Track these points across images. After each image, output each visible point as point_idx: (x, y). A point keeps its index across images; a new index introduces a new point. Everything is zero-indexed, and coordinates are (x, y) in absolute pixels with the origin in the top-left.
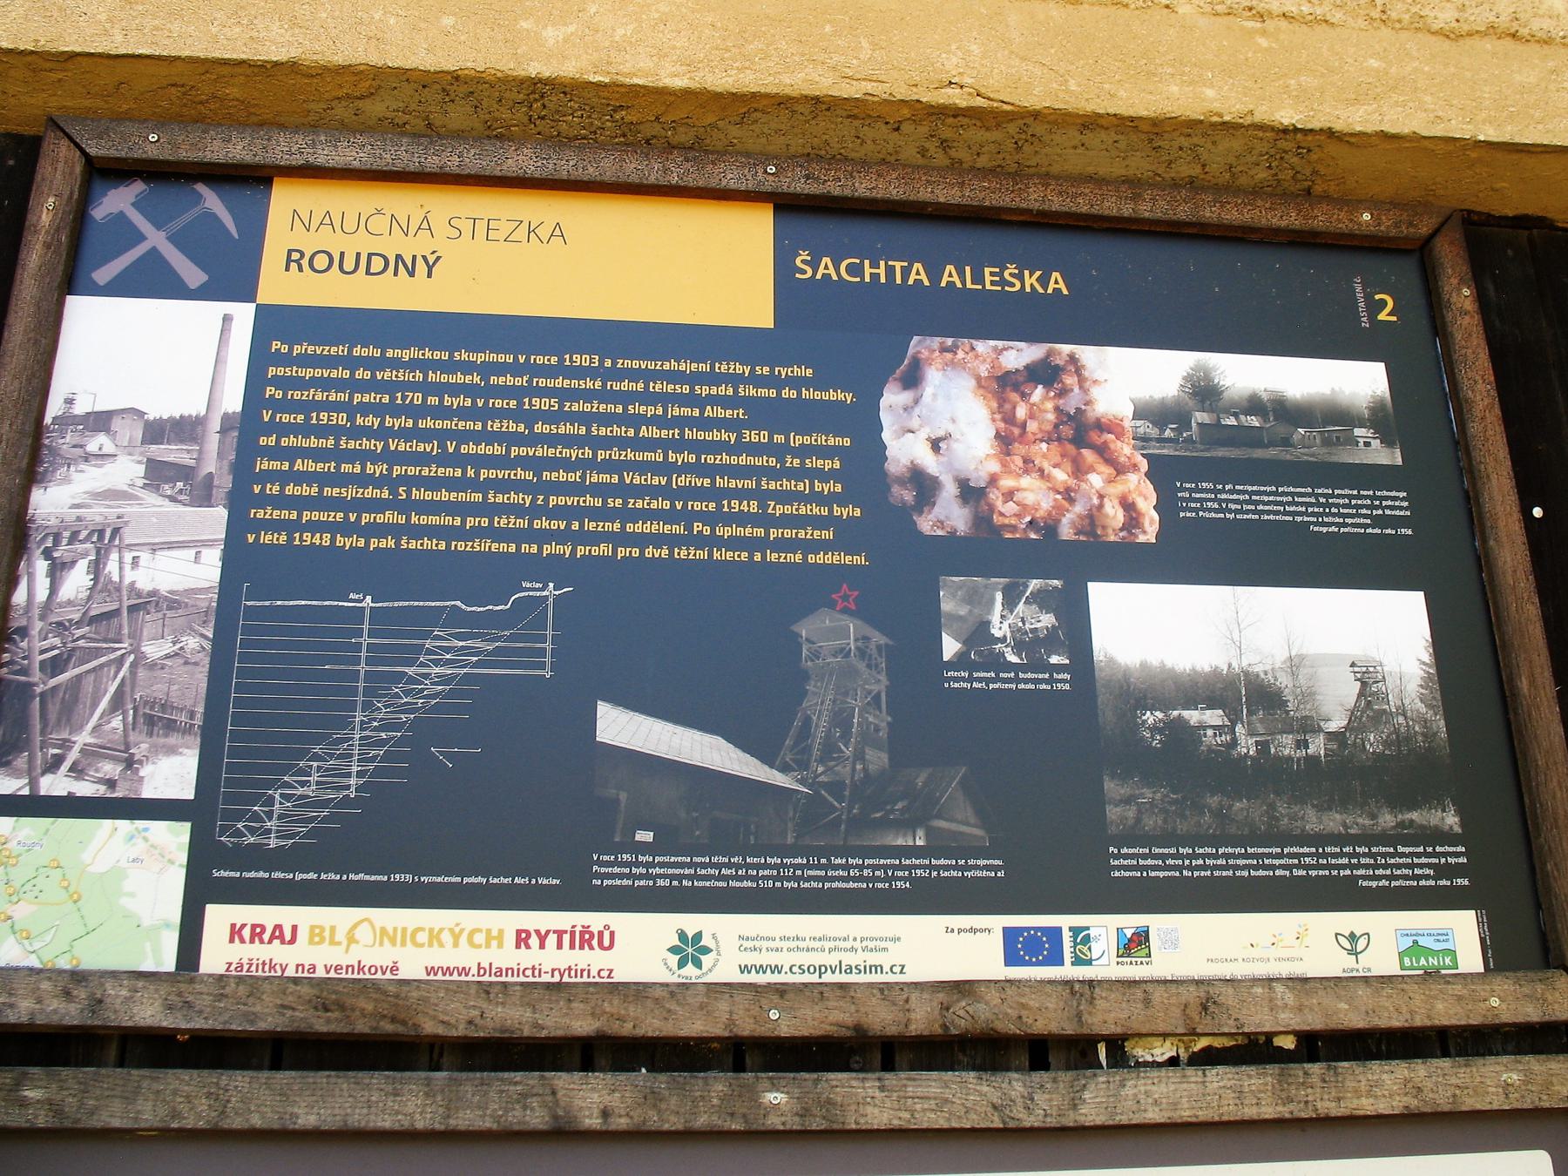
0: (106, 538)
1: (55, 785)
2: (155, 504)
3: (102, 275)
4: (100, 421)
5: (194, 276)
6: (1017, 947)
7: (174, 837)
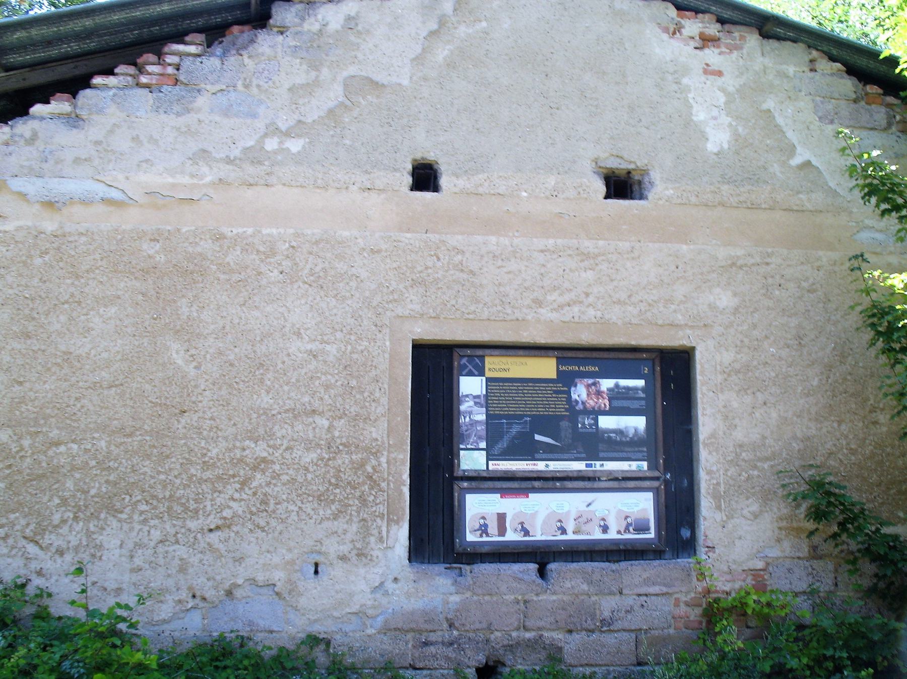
0: (470, 413)
1: (469, 446)
2: (476, 408)
3: (464, 373)
4: (467, 396)
5: (476, 373)
6: (587, 466)
7: (484, 453)
